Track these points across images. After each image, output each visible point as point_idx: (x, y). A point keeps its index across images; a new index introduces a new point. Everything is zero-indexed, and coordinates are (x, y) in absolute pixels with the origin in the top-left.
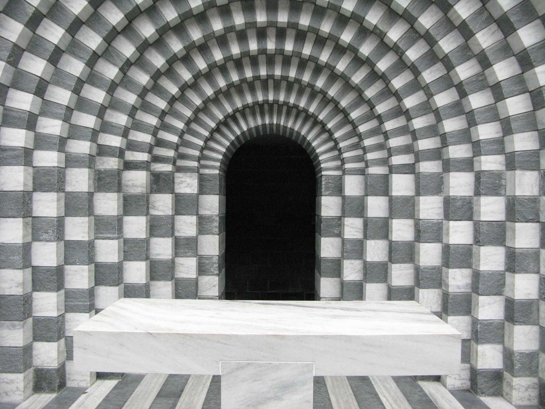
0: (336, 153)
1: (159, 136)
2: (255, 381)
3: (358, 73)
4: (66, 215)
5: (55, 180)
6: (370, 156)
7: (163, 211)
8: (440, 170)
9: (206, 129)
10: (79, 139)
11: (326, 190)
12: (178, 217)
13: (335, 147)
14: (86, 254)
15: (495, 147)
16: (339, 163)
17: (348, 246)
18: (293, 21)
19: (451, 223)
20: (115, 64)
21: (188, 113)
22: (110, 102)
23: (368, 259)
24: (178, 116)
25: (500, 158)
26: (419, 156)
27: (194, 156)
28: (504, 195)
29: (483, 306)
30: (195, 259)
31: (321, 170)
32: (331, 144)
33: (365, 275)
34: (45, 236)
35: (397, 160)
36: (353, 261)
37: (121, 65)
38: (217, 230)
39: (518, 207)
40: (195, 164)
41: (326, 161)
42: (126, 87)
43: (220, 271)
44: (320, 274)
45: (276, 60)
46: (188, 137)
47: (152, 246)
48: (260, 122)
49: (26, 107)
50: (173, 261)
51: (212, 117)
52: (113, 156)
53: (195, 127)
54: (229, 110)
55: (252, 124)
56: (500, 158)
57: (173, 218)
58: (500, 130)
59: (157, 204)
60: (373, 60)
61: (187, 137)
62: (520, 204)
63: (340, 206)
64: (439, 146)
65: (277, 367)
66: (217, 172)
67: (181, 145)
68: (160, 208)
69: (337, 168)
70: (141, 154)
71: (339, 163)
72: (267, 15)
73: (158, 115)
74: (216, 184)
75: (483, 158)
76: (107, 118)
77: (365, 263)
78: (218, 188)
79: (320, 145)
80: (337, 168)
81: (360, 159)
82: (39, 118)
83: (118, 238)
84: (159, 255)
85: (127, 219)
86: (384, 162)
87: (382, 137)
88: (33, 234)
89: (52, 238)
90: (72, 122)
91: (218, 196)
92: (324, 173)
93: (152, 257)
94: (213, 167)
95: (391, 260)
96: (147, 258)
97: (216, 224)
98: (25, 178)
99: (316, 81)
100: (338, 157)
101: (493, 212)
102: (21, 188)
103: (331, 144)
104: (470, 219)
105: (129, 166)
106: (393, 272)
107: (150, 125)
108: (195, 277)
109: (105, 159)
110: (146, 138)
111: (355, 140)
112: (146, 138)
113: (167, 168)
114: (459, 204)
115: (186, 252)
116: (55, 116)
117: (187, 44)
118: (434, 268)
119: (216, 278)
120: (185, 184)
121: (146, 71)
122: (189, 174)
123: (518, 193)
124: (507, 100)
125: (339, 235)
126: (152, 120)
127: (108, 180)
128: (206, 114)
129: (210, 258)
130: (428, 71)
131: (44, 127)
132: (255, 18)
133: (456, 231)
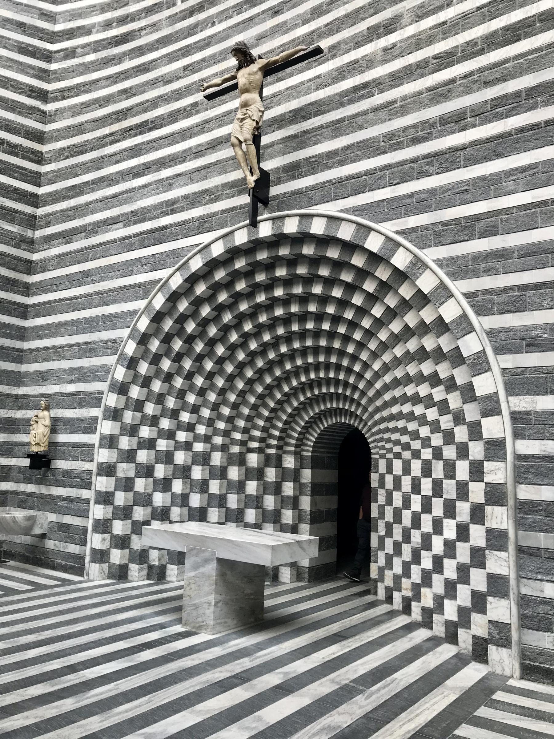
3: (371, 390)
4: (210, 478)
7: (270, 478)
11: (374, 469)
20: (235, 394)
27: (293, 444)
29: (424, 558)
45: (331, 383)
48: (334, 421)
49: (187, 420)
55: (330, 423)
70: (255, 443)
84: (267, 506)
88: (190, 488)
94: (308, 451)
97: (309, 489)
102: (183, 463)
120: (287, 462)
122: (290, 455)
129: (305, 511)
133: (415, 502)
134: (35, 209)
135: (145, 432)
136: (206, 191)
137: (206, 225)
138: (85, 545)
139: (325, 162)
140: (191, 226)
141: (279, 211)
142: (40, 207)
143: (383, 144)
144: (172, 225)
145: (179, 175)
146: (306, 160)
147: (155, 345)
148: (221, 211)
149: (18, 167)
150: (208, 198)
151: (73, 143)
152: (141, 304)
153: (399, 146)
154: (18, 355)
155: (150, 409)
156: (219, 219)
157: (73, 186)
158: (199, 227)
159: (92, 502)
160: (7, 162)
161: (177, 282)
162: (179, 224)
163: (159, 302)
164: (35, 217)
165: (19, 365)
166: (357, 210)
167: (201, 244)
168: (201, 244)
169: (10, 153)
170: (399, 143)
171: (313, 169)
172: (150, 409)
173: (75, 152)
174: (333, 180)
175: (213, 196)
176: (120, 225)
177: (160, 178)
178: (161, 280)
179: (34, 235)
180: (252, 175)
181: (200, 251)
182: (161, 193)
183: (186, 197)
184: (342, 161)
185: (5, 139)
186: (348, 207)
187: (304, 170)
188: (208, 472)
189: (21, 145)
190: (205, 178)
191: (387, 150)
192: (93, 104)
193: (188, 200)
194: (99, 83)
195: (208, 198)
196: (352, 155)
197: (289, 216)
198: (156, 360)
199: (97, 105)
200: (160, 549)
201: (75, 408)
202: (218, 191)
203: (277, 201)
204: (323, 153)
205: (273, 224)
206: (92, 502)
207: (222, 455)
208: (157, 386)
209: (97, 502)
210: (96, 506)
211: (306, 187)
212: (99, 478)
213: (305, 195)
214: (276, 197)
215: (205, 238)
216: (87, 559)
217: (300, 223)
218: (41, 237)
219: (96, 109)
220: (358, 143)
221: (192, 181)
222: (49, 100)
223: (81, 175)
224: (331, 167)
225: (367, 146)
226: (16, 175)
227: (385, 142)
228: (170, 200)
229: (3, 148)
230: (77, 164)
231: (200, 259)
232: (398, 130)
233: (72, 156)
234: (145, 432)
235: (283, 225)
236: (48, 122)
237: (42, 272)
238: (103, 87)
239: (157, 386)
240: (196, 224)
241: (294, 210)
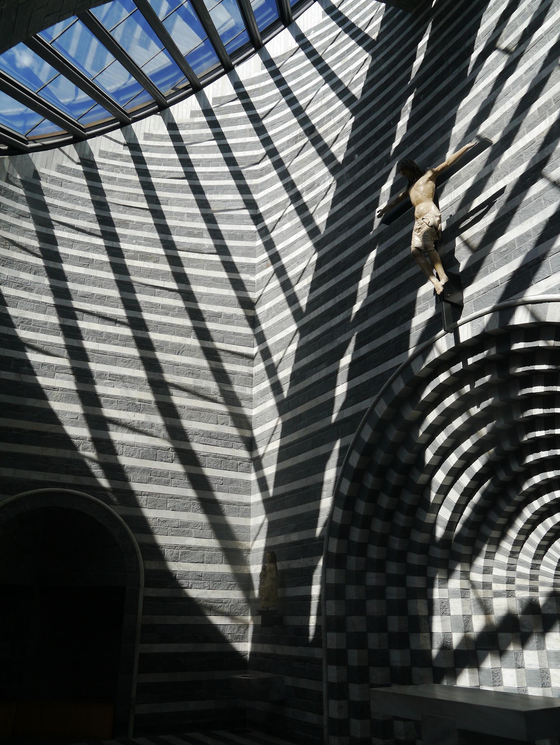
115: (557, 664)
134: (251, 368)
135: (372, 579)
138: (322, 714)
139: (517, 248)
142: (255, 365)
147: (370, 481)
149: (234, 333)
150: (402, 317)
151: (278, 302)
152: (350, 439)
154: (246, 510)
155: (374, 552)
157: (281, 339)
159: (324, 662)
160: (225, 331)
161: (382, 408)
163: (367, 434)
164: (251, 375)
165: (247, 519)
167: (401, 364)
168: (401, 364)
169: (227, 323)
172: (374, 552)
173: (281, 309)
174: (530, 262)
176: (323, 365)
178: (366, 410)
179: (252, 392)
180: (440, 281)
181: (400, 372)
185: (222, 312)
186: (553, 286)
188: (449, 623)
189: (235, 314)
192: (292, 263)
194: (295, 245)
198: (372, 497)
199: (296, 263)
200: (405, 720)
201: (300, 558)
203: (472, 301)
204: (513, 240)
206: (324, 662)
207: (462, 602)
208: (378, 526)
209: (329, 663)
210: (329, 667)
212: (329, 634)
216: (326, 731)
218: (258, 393)
219: (295, 267)
221: (385, 306)
222: (256, 272)
223: (287, 328)
226: (233, 341)
229: (221, 320)
230: (283, 319)
231: (402, 380)
233: (278, 313)
234: (372, 579)
236: (257, 289)
237: (261, 425)
238: (299, 247)
239: (378, 526)
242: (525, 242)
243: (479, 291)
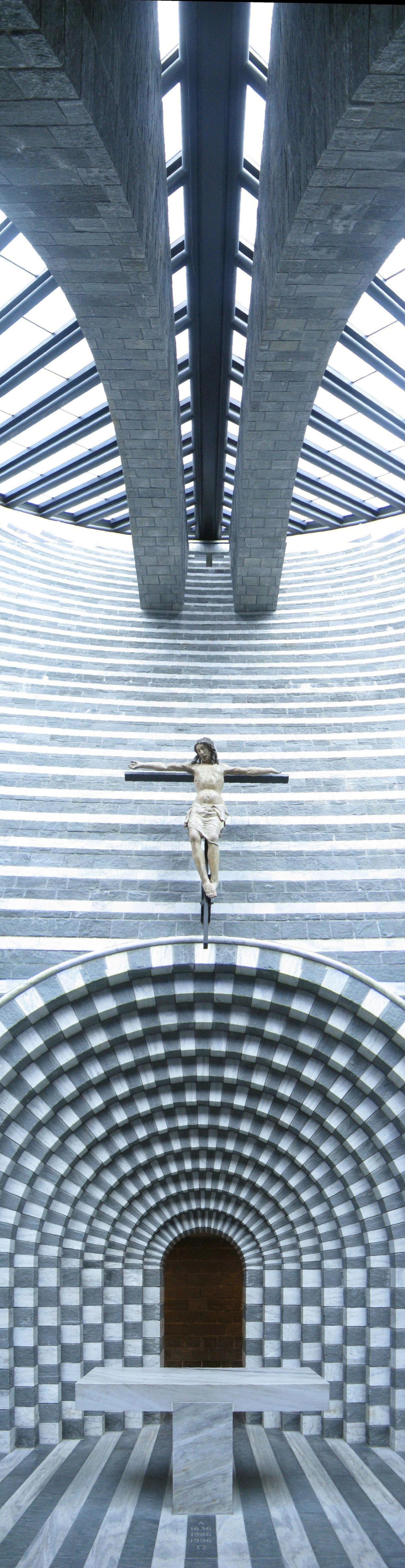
0: (258, 1251)
1: (111, 1239)
2: (195, 1415)
5: (31, 1278)
6: (285, 1255)
8: (341, 1267)
9: (149, 1233)
10: (49, 1245)
12: (126, 1306)
13: (257, 1246)
14: (56, 1337)
15: (382, 1249)
16: (260, 1259)
17: (268, 1329)
18: (220, 1147)
19: (349, 1309)
21: (135, 1220)
22: (73, 1213)
23: (284, 1339)
24: (126, 1222)
25: (385, 1258)
26: (324, 1255)
28: (389, 1287)
30: (141, 1340)
31: (245, 1266)
32: (253, 1244)
33: (282, 1352)
34: (24, 1322)
35: (307, 1258)
36: (272, 1341)
37: (82, 1184)
38: (159, 1316)
39: (397, 1297)
40: (140, 1262)
41: (250, 1258)
42: (86, 1202)
43: (161, 1351)
44: (245, 1352)
46: (134, 1240)
47: (106, 1330)
50: (123, 1343)
51: (154, 1222)
52: (76, 1257)
53: (140, 1231)
54: (169, 1216)
56: (385, 1258)
57: (122, 1307)
58: (386, 1235)
59: (110, 1296)
60: (286, 1177)
61: (134, 1239)
62: (399, 1294)
63: (261, 1295)
64: (340, 1247)
65: (209, 1406)
66: (158, 1268)
67: (129, 1246)
68: (113, 1299)
69: (259, 1264)
71: (260, 1259)
72: (200, 1142)
73: (111, 1223)
74: (158, 1278)
75: (372, 1258)
76: (70, 1226)
77: (282, 1343)
78: (159, 1281)
79: (244, 1245)
80: (259, 1264)
81: (278, 1256)
82: (19, 1228)
83: (80, 1324)
85: (86, 1308)
86: (297, 1259)
87: (294, 1238)
89: (30, 1324)
90: (43, 1231)
91: (159, 1288)
92: (247, 1268)
93: (105, 1339)
95: (303, 1340)
96: (102, 1340)
98: (10, 1277)
99: (240, 1193)
100: (260, 1255)
101: (380, 1301)
103: (253, 1244)
104: (363, 1306)
105: (87, 1265)
106: (304, 1350)
107: (105, 1232)
108: (141, 1355)
109: (69, 1260)
110: (100, 1242)
111: (273, 1241)
112: (100, 1242)
113: (118, 1266)
114: (354, 1294)
116: (32, 1227)
117: (135, 1166)
118: (336, 1346)
119: (158, 1357)
121: (102, 1188)
123: (397, 1286)
124: (388, 1213)
125: (261, 1319)
126: (106, 1227)
127: (72, 1277)
128: (149, 1221)
130: (329, 1188)
131: (23, 1236)
132: (190, 1144)
136: (96, 882)
137: (98, 927)
139: (286, 892)
140: (68, 922)
141: (226, 934)
143: (360, 890)
144: (31, 913)
145: (43, 850)
146: (258, 883)
148: (127, 914)
153: (379, 897)
156: (122, 924)
158: (83, 927)
162: (46, 915)
166: (344, 957)
167: (90, 952)
168: (85, 952)
170: (381, 894)
171: (269, 896)
175: (108, 892)
177: (6, 845)
182: (6, 865)
183: (55, 881)
184: (311, 896)
187: (257, 893)
190: (90, 865)
191: (368, 898)
193: (62, 886)
195: (98, 891)
196: (323, 893)
197: (244, 944)
202: (117, 887)
203: (223, 922)
205: (218, 950)
211: (267, 915)
213: (266, 924)
214: (223, 916)
215: (96, 946)
217: (261, 957)
220: (329, 882)
224: (296, 900)
225: (341, 888)
227: (363, 889)
228: (29, 878)
232: (377, 881)
235: (235, 954)
240: (80, 922)
241: (251, 938)
242: (296, 890)
243: (235, 915)
